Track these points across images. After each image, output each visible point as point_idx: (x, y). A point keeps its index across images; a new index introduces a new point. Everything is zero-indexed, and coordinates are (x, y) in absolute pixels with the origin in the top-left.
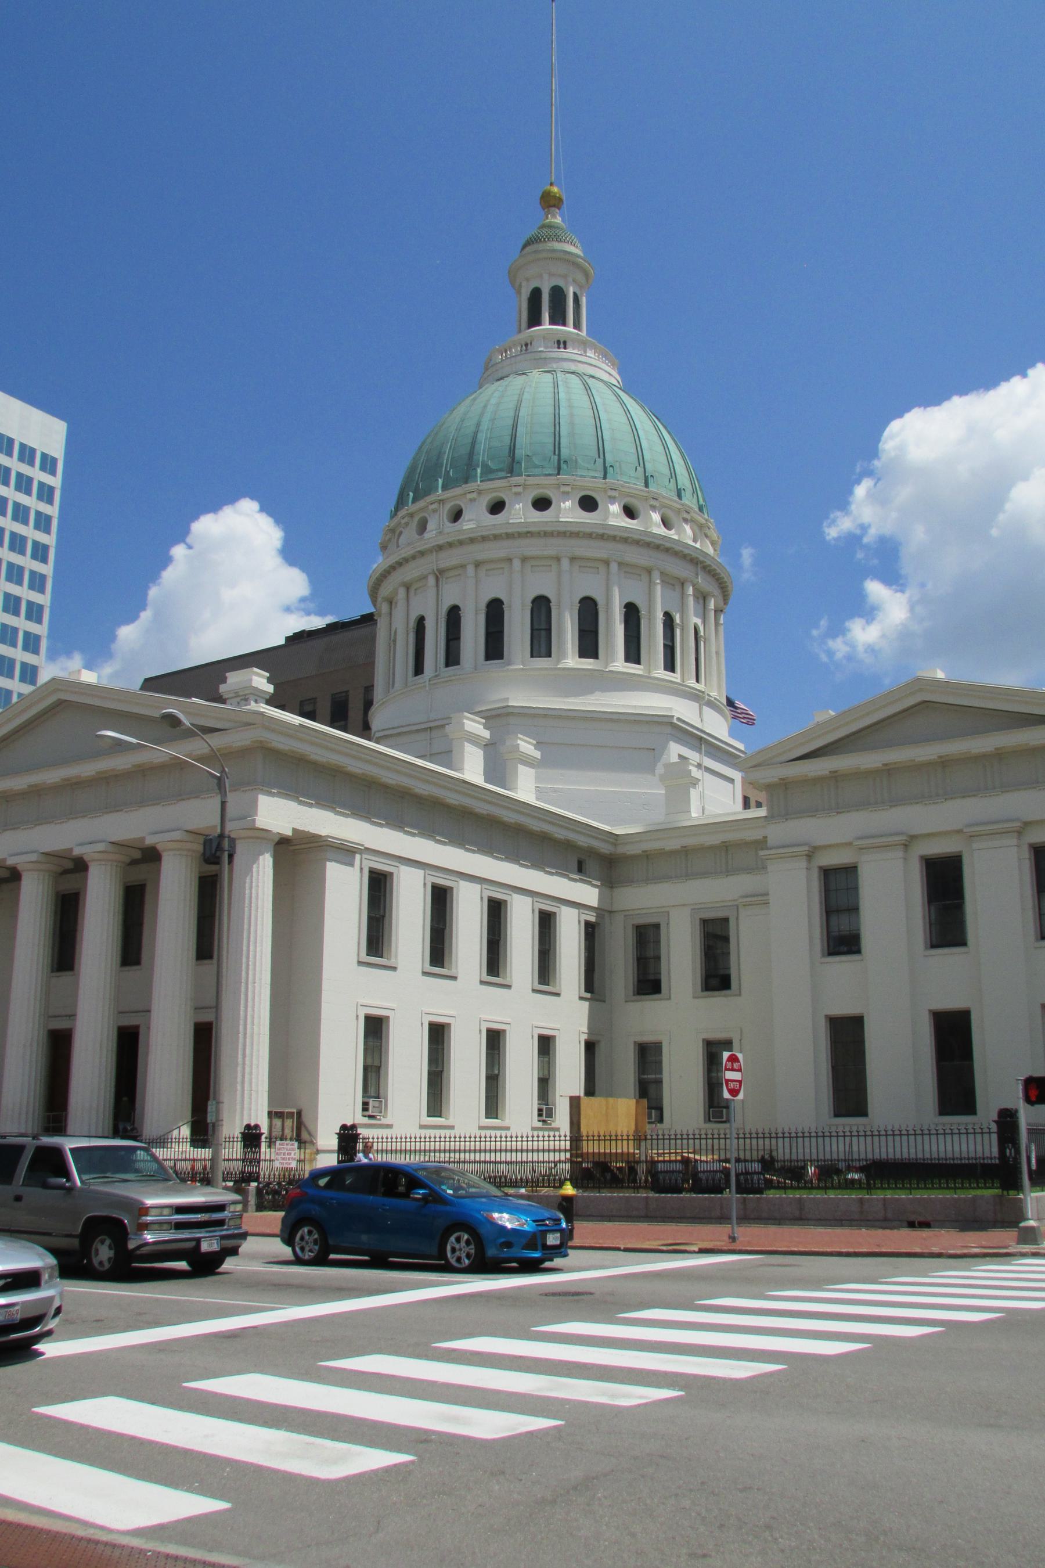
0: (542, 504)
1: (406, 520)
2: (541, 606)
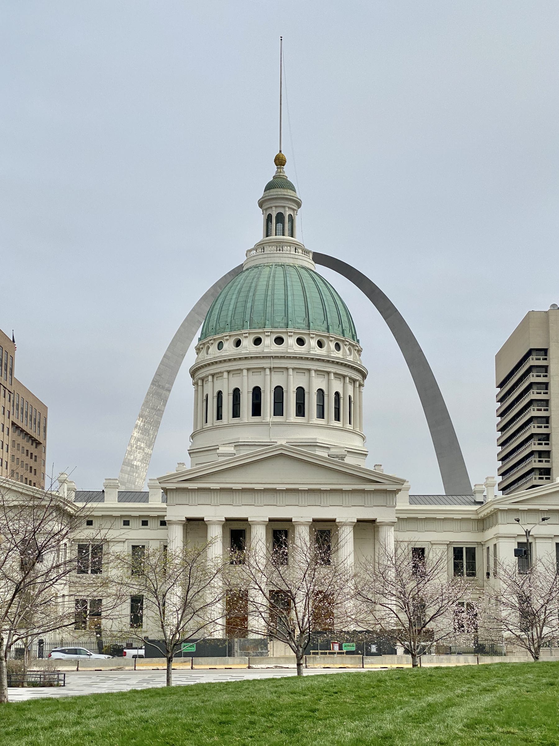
0: (279, 341)
1: (212, 342)
2: (279, 392)
